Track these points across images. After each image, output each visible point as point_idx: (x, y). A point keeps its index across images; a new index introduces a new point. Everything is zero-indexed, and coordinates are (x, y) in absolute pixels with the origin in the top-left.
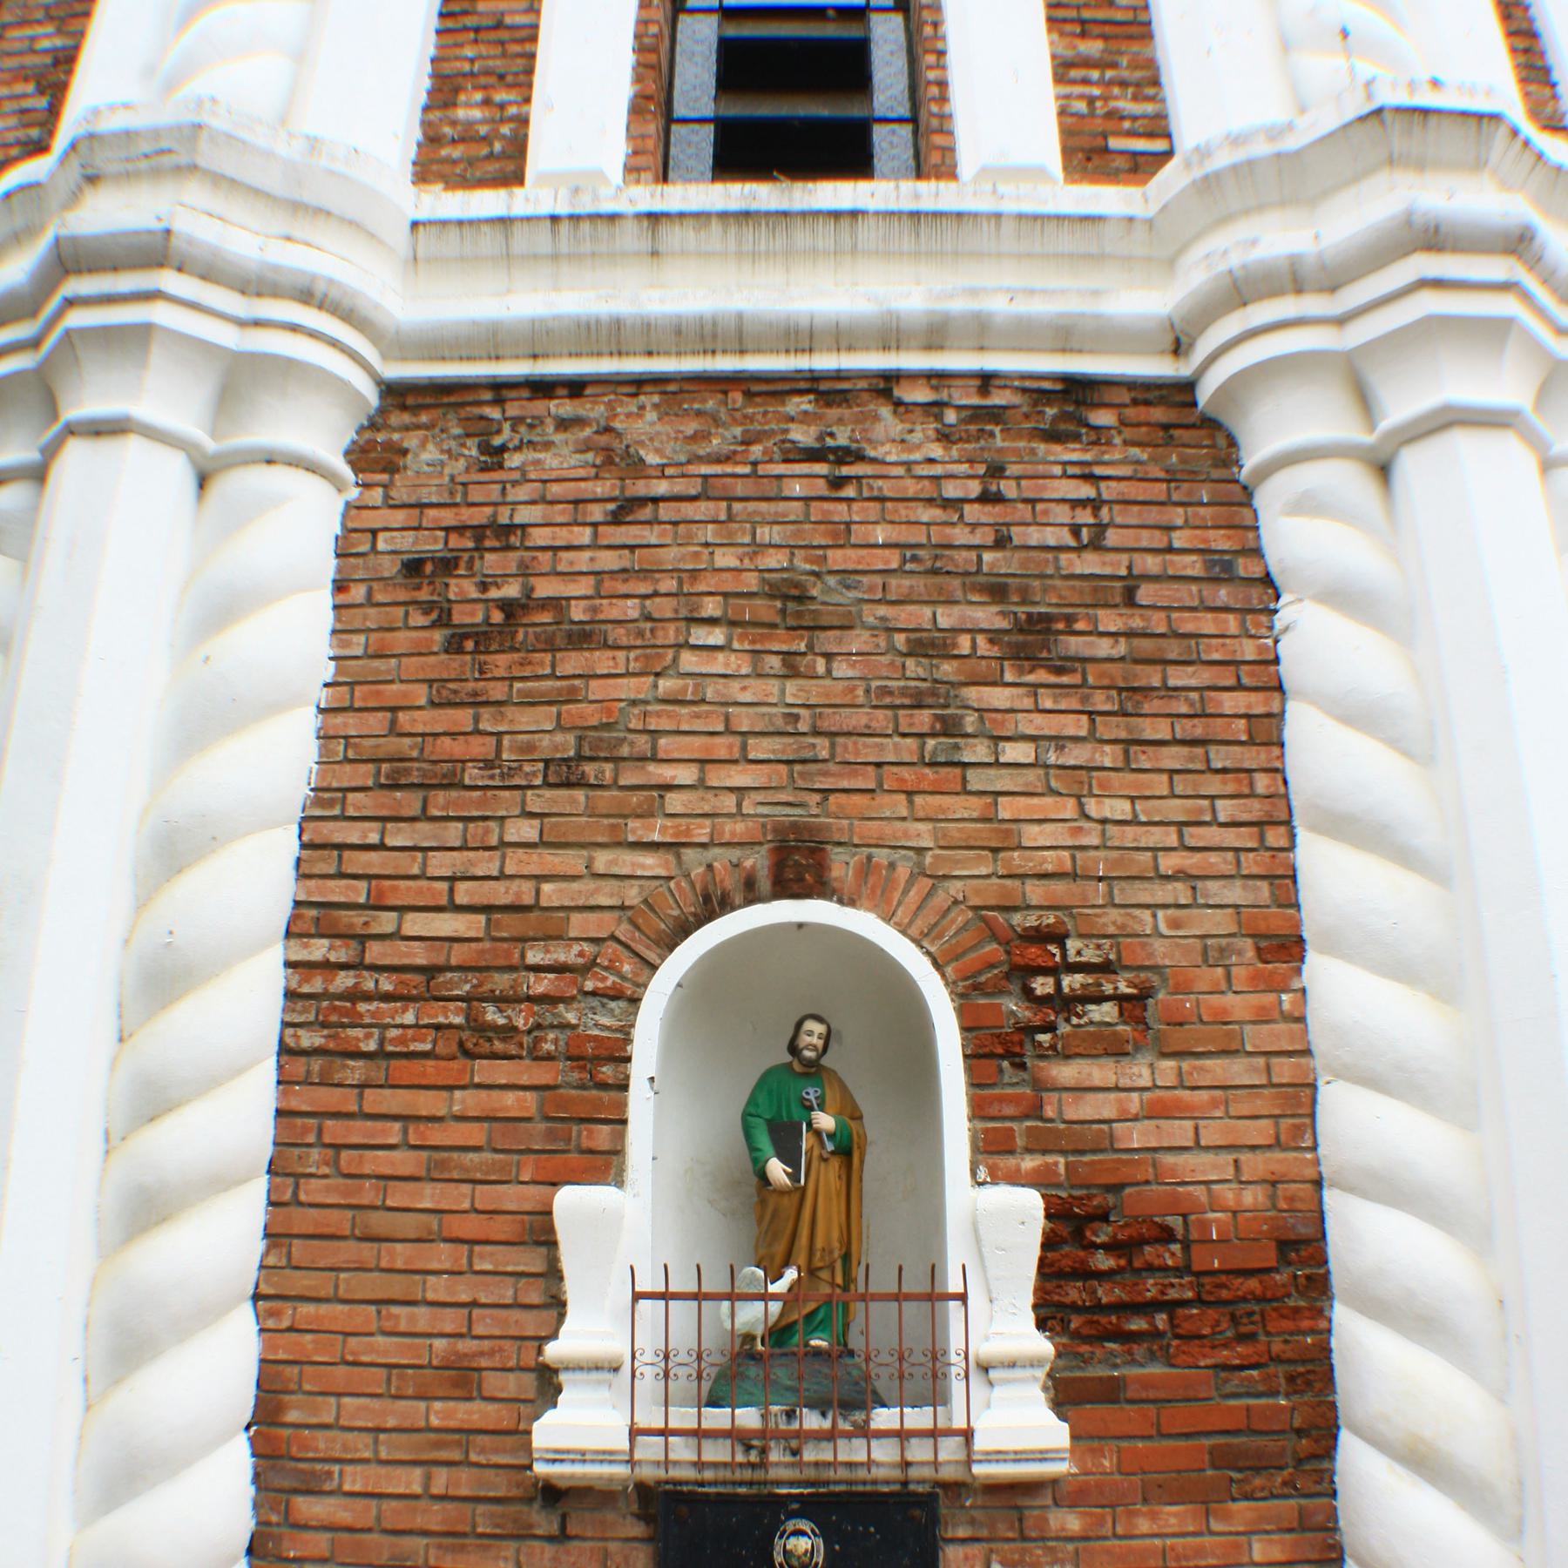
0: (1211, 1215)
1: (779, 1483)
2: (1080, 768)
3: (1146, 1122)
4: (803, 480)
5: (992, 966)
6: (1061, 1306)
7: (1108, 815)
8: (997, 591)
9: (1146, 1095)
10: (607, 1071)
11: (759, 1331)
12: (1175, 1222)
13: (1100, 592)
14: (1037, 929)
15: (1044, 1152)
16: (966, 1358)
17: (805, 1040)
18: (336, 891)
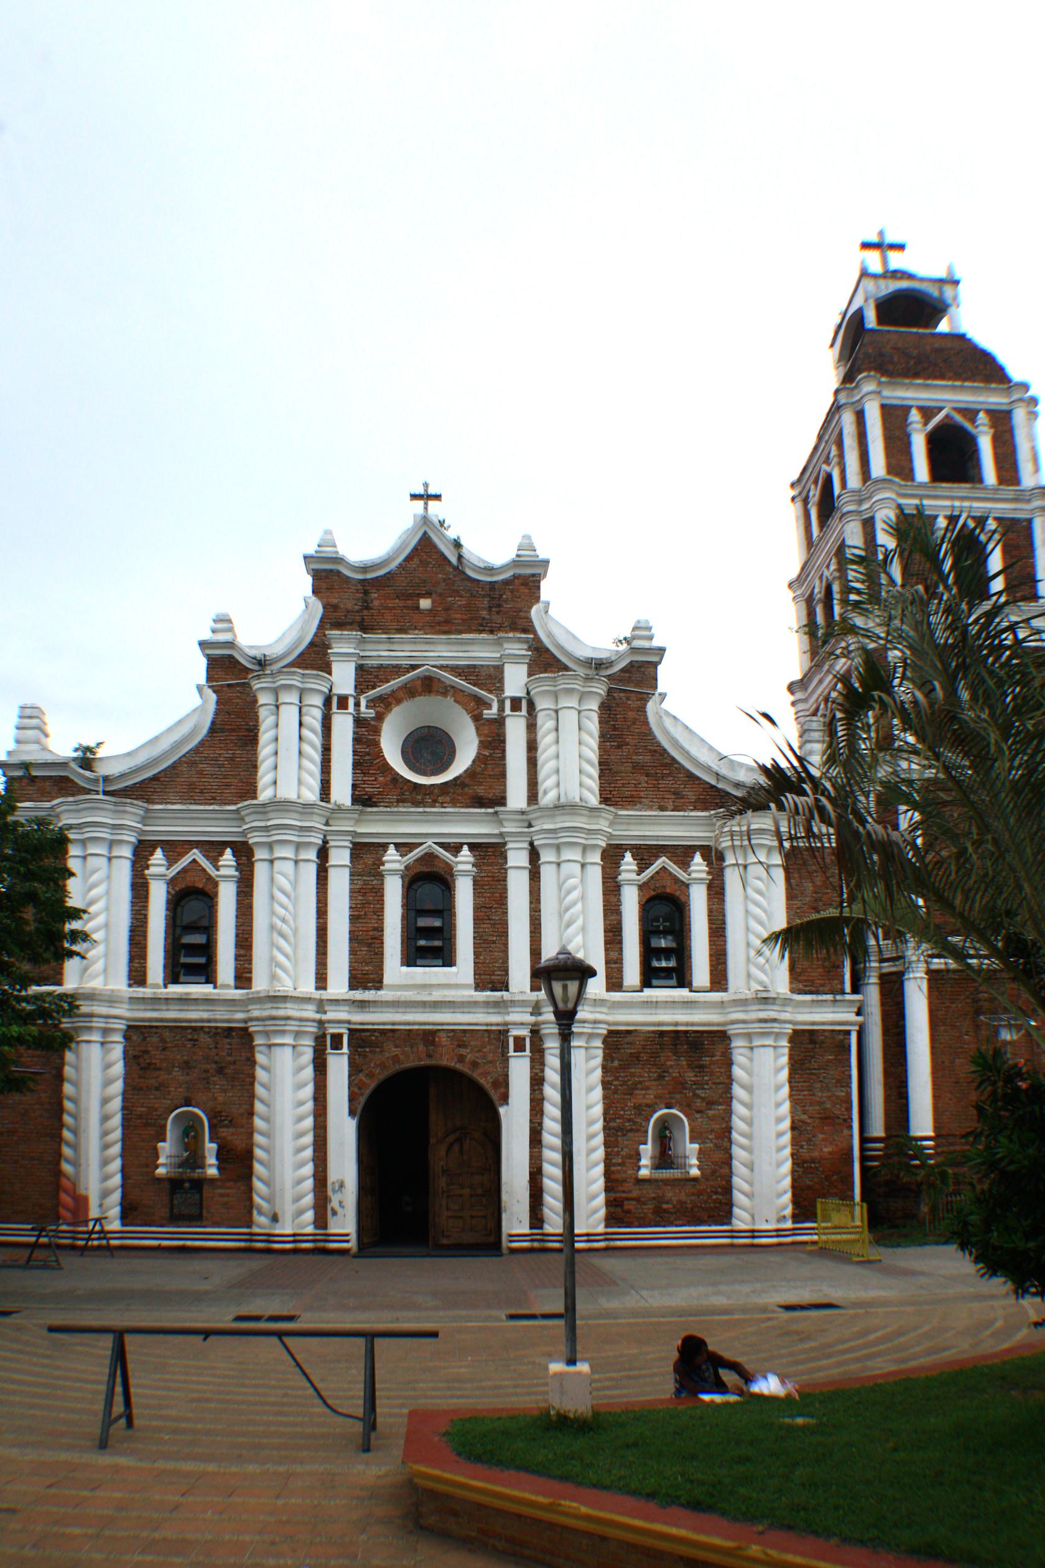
8: (216, 1063)
13: (230, 1063)
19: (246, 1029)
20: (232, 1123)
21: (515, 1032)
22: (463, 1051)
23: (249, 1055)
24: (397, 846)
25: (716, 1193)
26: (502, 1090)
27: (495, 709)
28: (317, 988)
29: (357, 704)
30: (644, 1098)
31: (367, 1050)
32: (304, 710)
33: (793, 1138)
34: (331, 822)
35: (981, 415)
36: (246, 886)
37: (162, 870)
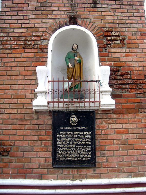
0: (134, 71)
1: (71, 110)
2: (114, 8)
3: (125, 57)
5: (101, 35)
6: (113, 84)
7: (118, 15)
9: (124, 54)
10: (45, 50)
11: (68, 88)
12: (129, 72)
14: (108, 30)
15: (110, 61)
16: (99, 90)
17: (74, 47)
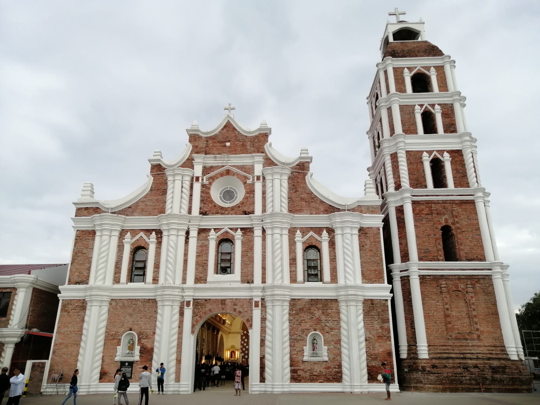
4: (134, 306)
18: (108, 331)
19: (155, 299)
20: (147, 337)
21: (255, 299)
22: (236, 307)
23: (155, 310)
24: (215, 229)
25: (335, 368)
26: (250, 323)
27: (251, 180)
28: (183, 283)
29: (203, 180)
30: (305, 326)
31: (200, 307)
32: (183, 182)
33: (366, 345)
34: (191, 221)
35: (432, 68)
36: (159, 245)
37: (129, 240)
